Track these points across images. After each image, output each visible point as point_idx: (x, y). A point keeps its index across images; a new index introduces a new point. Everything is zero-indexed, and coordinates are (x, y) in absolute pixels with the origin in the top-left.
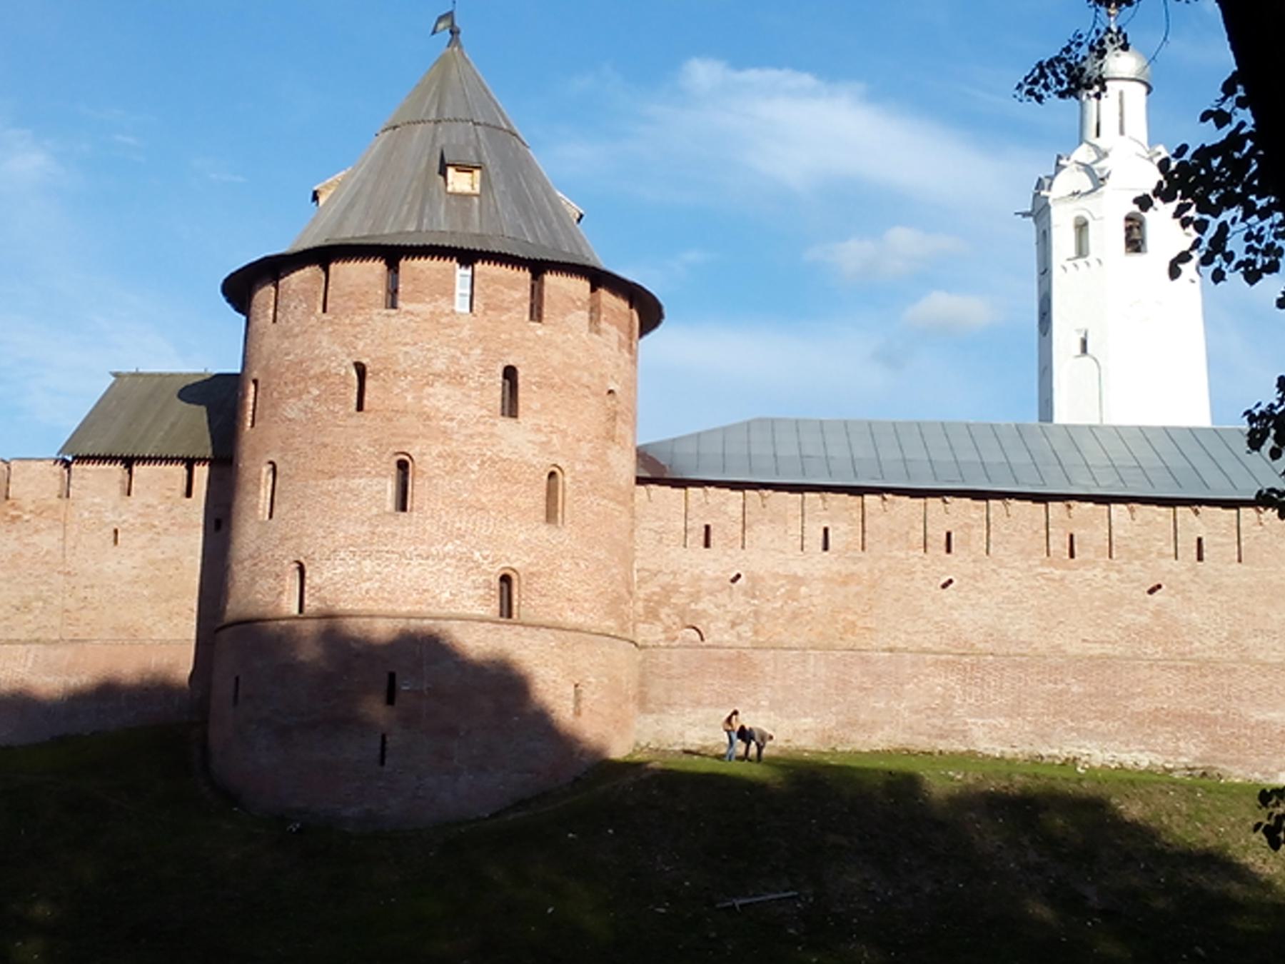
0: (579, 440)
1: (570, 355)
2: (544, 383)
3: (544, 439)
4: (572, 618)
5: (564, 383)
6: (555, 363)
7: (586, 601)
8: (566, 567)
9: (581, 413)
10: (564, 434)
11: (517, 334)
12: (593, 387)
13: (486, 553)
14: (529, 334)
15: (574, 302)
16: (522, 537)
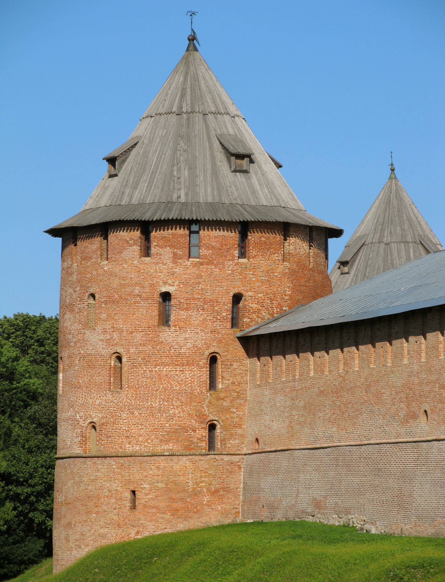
0: (132, 333)
1: (124, 279)
2: (110, 301)
3: (108, 337)
4: (129, 448)
5: (121, 297)
6: (115, 286)
7: (140, 436)
8: (124, 416)
9: (134, 314)
10: (121, 331)
11: (94, 273)
12: (144, 295)
13: (82, 414)
14: (100, 271)
15: (127, 242)
16: (98, 402)
